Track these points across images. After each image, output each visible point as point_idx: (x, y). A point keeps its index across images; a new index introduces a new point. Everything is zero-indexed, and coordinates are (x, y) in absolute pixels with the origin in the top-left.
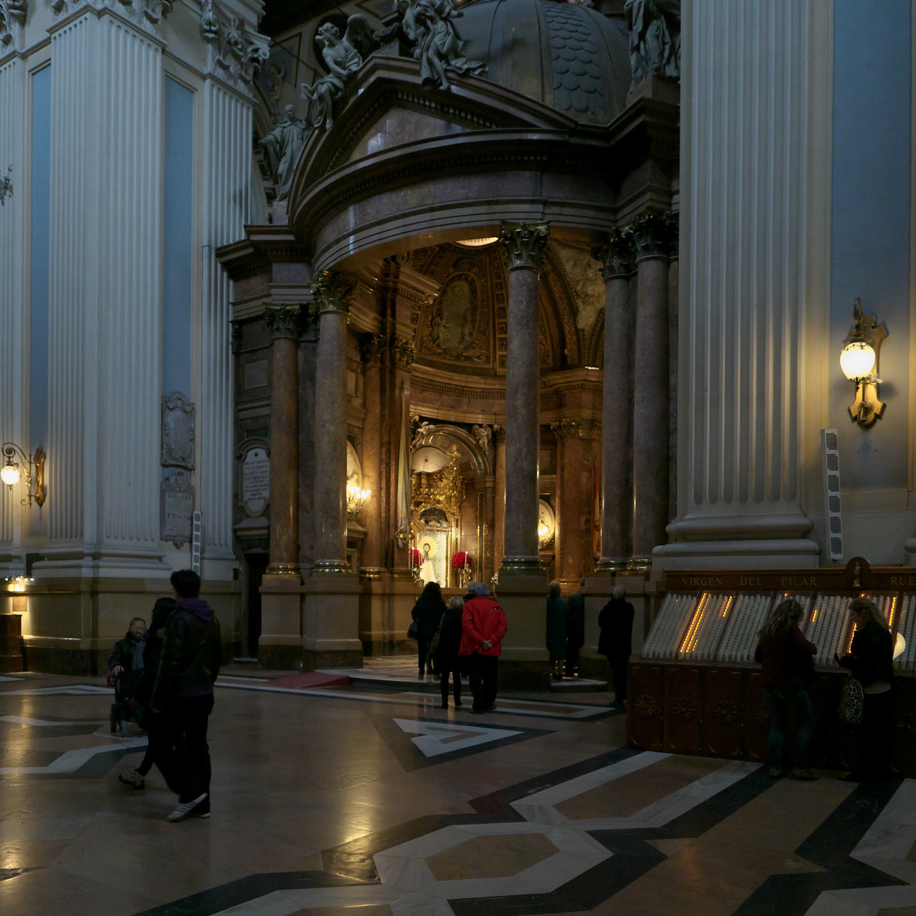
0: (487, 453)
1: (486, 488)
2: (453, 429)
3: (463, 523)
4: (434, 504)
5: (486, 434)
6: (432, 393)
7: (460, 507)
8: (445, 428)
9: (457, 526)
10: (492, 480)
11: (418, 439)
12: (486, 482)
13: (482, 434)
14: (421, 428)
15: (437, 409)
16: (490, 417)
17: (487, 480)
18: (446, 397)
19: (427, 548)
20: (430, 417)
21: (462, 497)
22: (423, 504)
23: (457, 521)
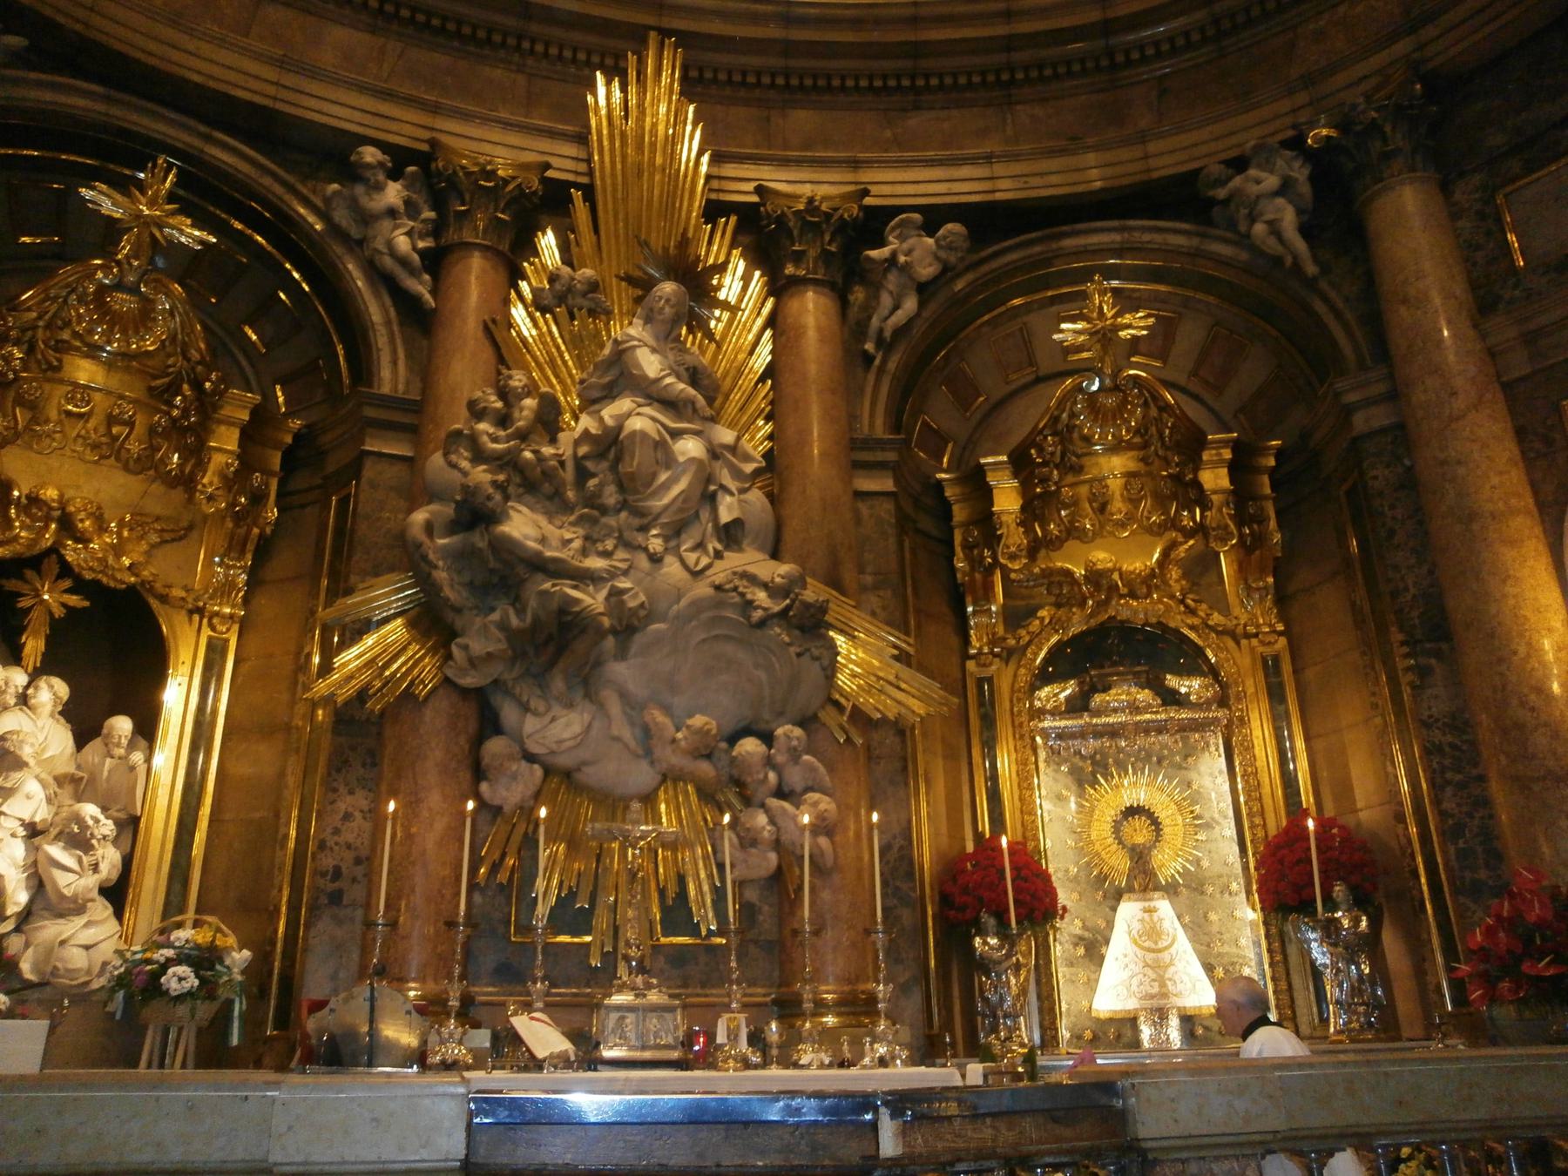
0: (1311, 269)
1: (1355, 440)
2: (1117, 237)
3: (1310, 674)
4: (1102, 605)
5: (1271, 181)
6: (955, 113)
7: (1282, 600)
8: (1068, 243)
9: (1275, 694)
10: (1380, 388)
11: (886, 300)
12: (1349, 411)
13: (1254, 189)
14: (880, 243)
15: (989, 159)
16: (1285, 105)
17: (1352, 398)
18: (1038, 111)
19: (1139, 833)
20: (948, 200)
21: (1260, 539)
22: (1043, 613)
23: (1270, 668)
